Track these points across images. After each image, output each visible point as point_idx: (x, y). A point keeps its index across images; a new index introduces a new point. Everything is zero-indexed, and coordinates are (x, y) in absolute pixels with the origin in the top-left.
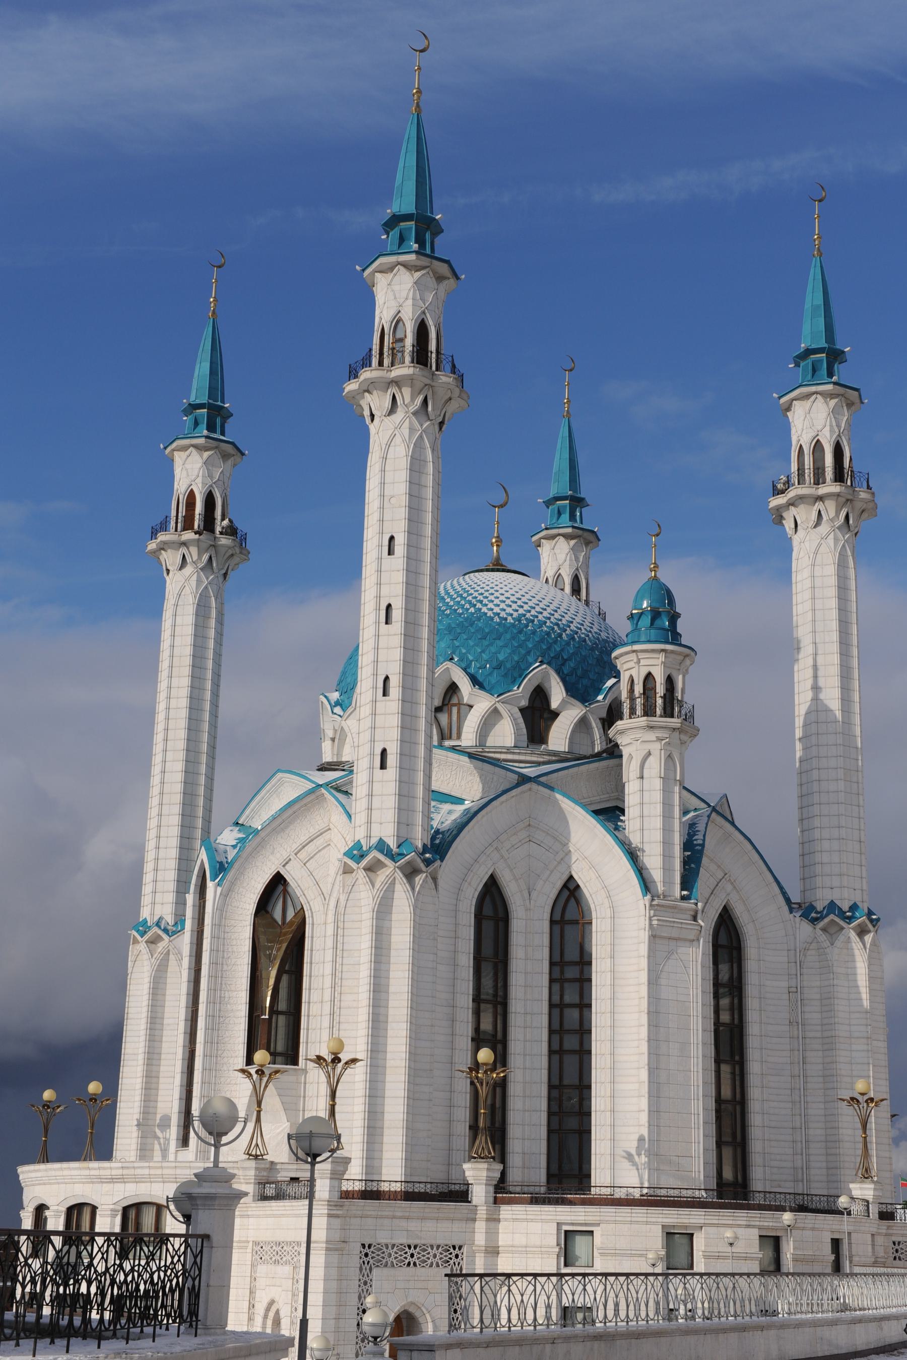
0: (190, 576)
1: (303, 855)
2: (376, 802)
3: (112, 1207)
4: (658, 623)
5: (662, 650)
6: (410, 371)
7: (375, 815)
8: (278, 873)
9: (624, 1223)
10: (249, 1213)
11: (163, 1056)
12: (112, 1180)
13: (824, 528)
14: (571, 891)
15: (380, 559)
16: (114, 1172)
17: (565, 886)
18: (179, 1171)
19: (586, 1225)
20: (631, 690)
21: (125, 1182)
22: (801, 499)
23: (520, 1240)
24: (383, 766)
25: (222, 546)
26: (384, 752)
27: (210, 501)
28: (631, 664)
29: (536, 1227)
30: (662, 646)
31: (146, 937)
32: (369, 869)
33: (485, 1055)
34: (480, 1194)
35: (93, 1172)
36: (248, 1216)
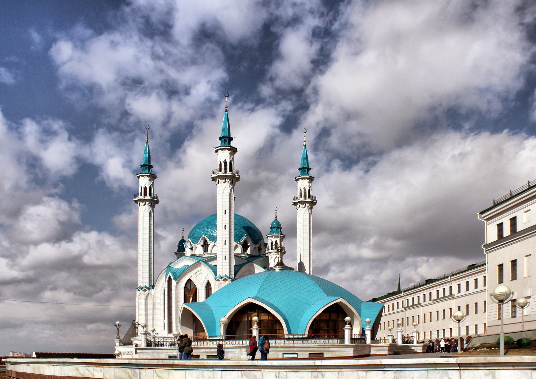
2: (224, 267)
7: (224, 270)
20: (272, 244)
24: (225, 259)
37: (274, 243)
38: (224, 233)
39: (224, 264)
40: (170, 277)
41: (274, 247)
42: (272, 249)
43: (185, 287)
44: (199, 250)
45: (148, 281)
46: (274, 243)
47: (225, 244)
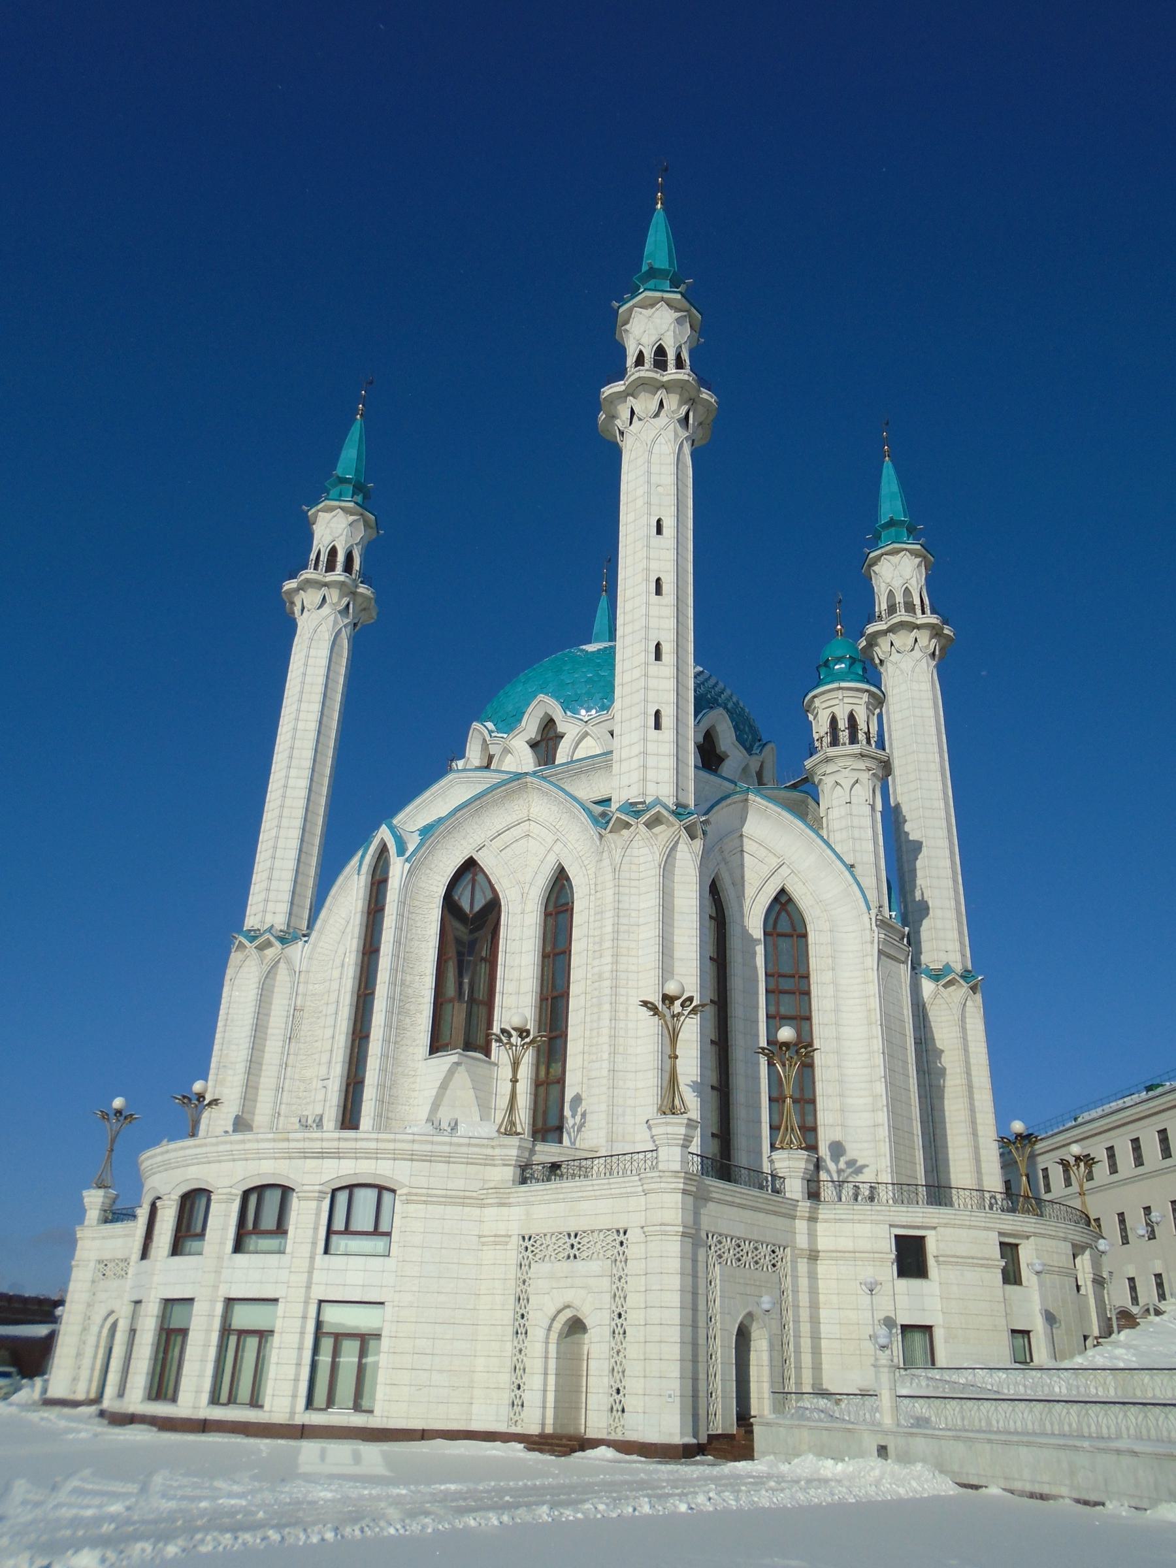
0: (328, 616)
1: (498, 843)
3: (317, 1188)
4: (853, 669)
5: (867, 691)
6: (686, 377)
7: (651, 775)
8: (471, 858)
9: (961, 1226)
10: (511, 1200)
11: (264, 1067)
12: (322, 1155)
13: (917, 653)
14: (782, 902)
15: (648, 537)
16: (325, 1144)
17: (776, 899)
18: (416, 1147)
19: (918, 1228)
21: (339, 1158)
22: (902, 625)
23: (845, 1244)
24: (658, 726)
25: (362, 594)
26: (657, 714)
27: (349, 557)
28: (836, 702)
29: (864, 1229)
30: (866, 686)
31: (257, 943)
32: (649, 825)
33: (786, 1033)
34: (794, 1188)
35: (293, 1145)
36: (508, 1205)
37: (842, 724)
38: (654, 611)
39: (651, 747)
40: (383, 849)
41: (844, 736)
42: (835, 742)
43: (450, 904)
44: (518, 755)
45: (284, 907)
46: (842, 724)
47: (658, 657)
